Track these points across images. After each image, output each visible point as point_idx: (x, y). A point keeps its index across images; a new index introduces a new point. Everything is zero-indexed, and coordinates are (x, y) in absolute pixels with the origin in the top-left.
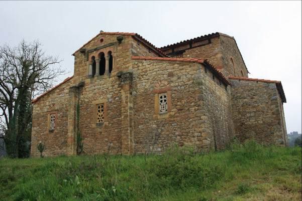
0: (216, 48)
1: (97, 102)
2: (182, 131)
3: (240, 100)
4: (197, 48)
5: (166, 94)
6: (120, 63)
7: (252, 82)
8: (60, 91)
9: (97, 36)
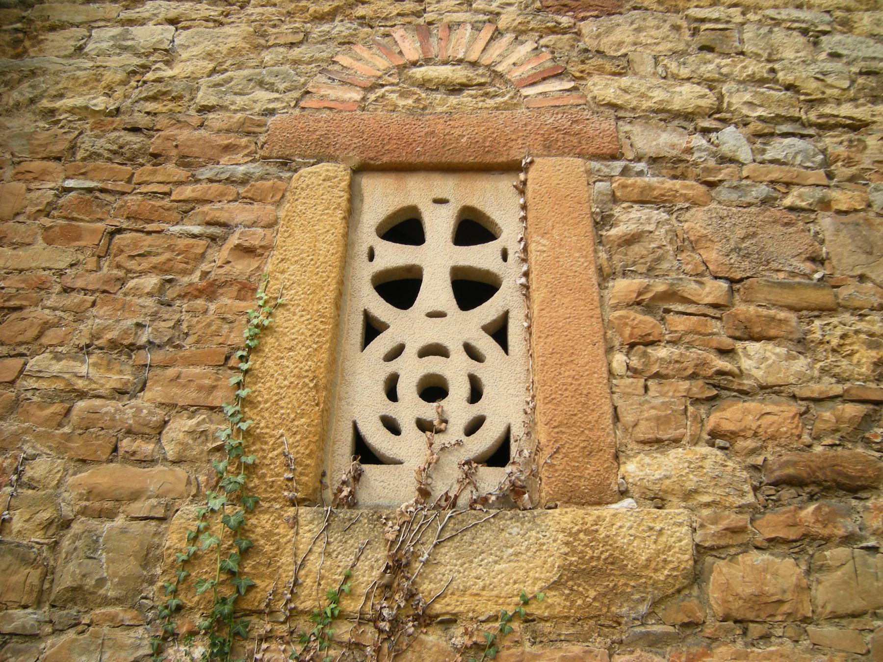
5: (495, 199)
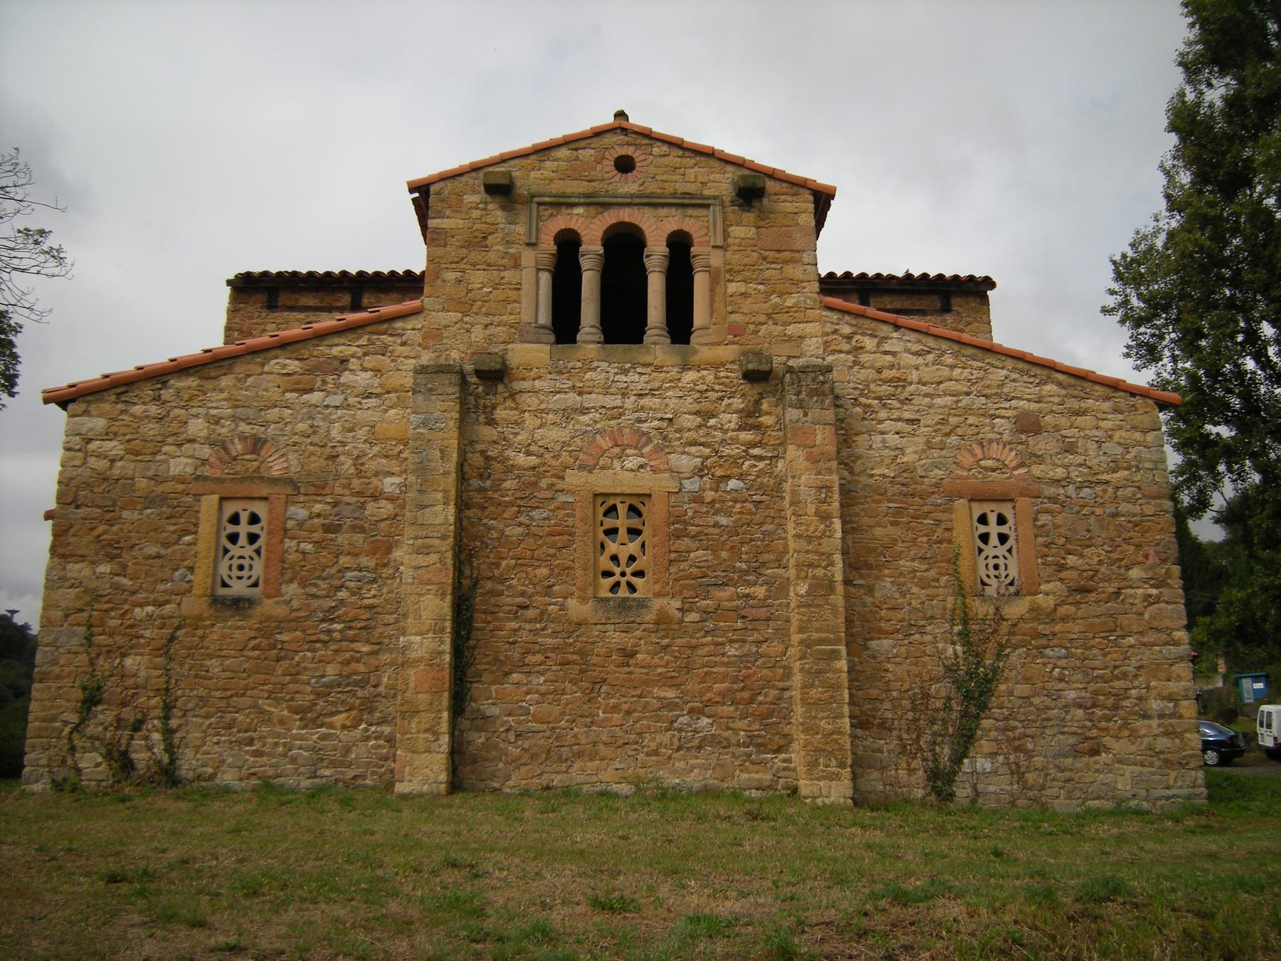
1: (602, 481)
2: (1092, 687)
5: (1007, 510)
6: (747, 306)
8: (309, 371)
9: (598, 133)
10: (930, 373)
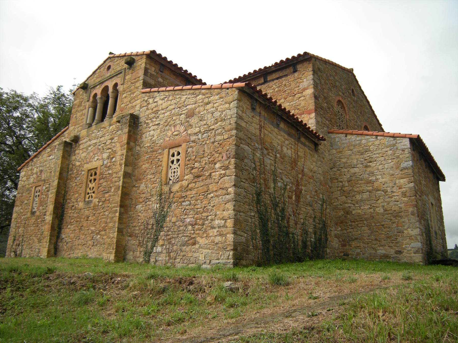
0: (305, 80)
2: (196, 216)
3: (346, 170)
4: (275, 81)
5: (180, 149)
6: (125, 100)
7: (368, 137)
8: (51, 151)
9: (105, 62)
10: (164, 106)
